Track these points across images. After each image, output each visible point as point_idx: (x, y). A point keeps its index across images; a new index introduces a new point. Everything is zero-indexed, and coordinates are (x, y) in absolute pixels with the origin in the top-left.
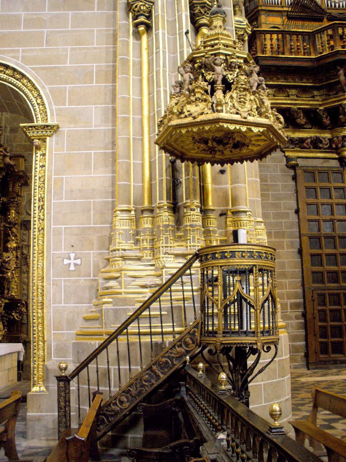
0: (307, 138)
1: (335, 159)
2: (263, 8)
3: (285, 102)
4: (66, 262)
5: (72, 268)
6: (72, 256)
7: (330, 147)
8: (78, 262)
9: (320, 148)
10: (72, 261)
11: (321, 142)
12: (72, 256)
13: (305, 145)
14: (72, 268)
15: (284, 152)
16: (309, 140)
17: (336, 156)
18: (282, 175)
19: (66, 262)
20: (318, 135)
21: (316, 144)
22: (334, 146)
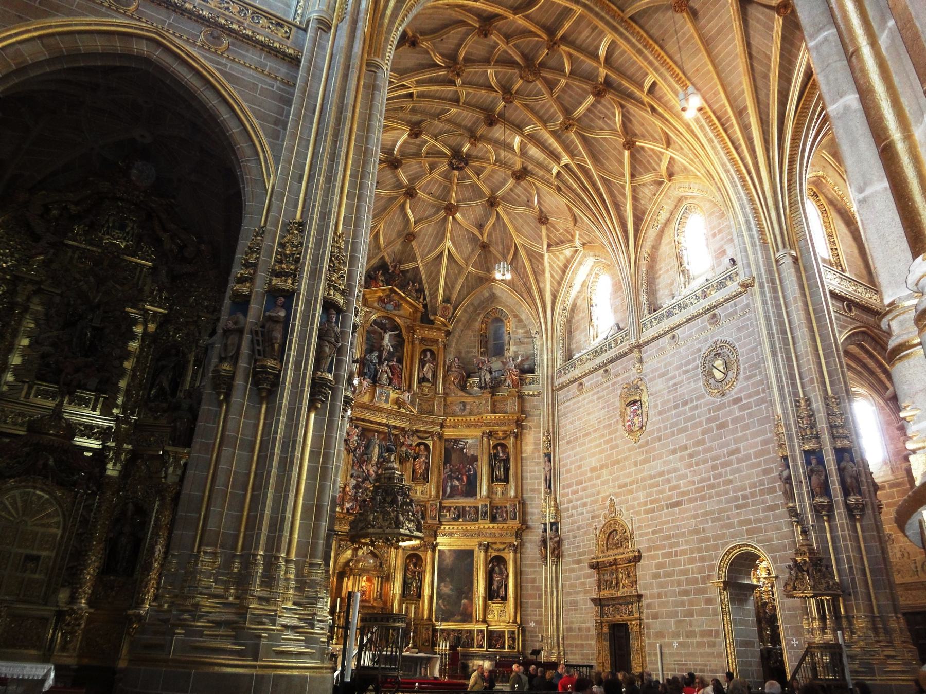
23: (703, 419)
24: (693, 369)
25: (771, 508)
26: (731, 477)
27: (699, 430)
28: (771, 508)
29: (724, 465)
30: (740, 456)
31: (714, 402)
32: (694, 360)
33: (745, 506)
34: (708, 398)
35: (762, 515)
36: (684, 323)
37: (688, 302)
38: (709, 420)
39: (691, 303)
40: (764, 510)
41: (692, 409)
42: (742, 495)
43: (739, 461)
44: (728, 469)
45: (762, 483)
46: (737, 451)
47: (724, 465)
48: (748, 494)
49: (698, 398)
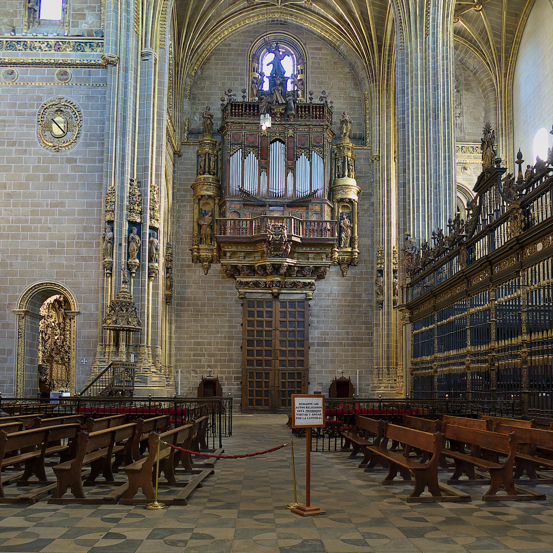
0: (251, 282)
1: (270, 293)
2: (228, 199)
3: (234, 262)
4: (82, 361)
5: (84, 363)
6: (84, 359)
7: (266, 287)
8: (86, 361)
9: (260, 287)
10: (84, 361)
11: (260, 283)
12: (84, 359)
13: (250, 285)
14: (84, 363)
15: (238, 289)
16: (252, 283)
17: (271, 291)
18: (236, 303)
19: (82, 361)
20: (258, 279)
21: (256, 285)
22: (268, 286)
23: (31, 166)
24: (28, 115)
25: (84, 259)
26: (50, 225)
27: (24, 174)
28: (84, 259)
29: (44, 213)
30: (63, 209)
31: (46, 154)
32: (32, 106)
33: (60, 252)
34: (40, 148)
35: (74, 263)
36: (29, 64)
37: (37, 44)
38: (36, 168)
39: (40, 48)
40: (77, 259)
41: (18, 152)
42: (58, 243)
43: (61, 213)
44: (49, 218)
45: (80, 237)
46: (62, 204)
47: (44, 213)
48: (65, 243)
49: (28, 144)
